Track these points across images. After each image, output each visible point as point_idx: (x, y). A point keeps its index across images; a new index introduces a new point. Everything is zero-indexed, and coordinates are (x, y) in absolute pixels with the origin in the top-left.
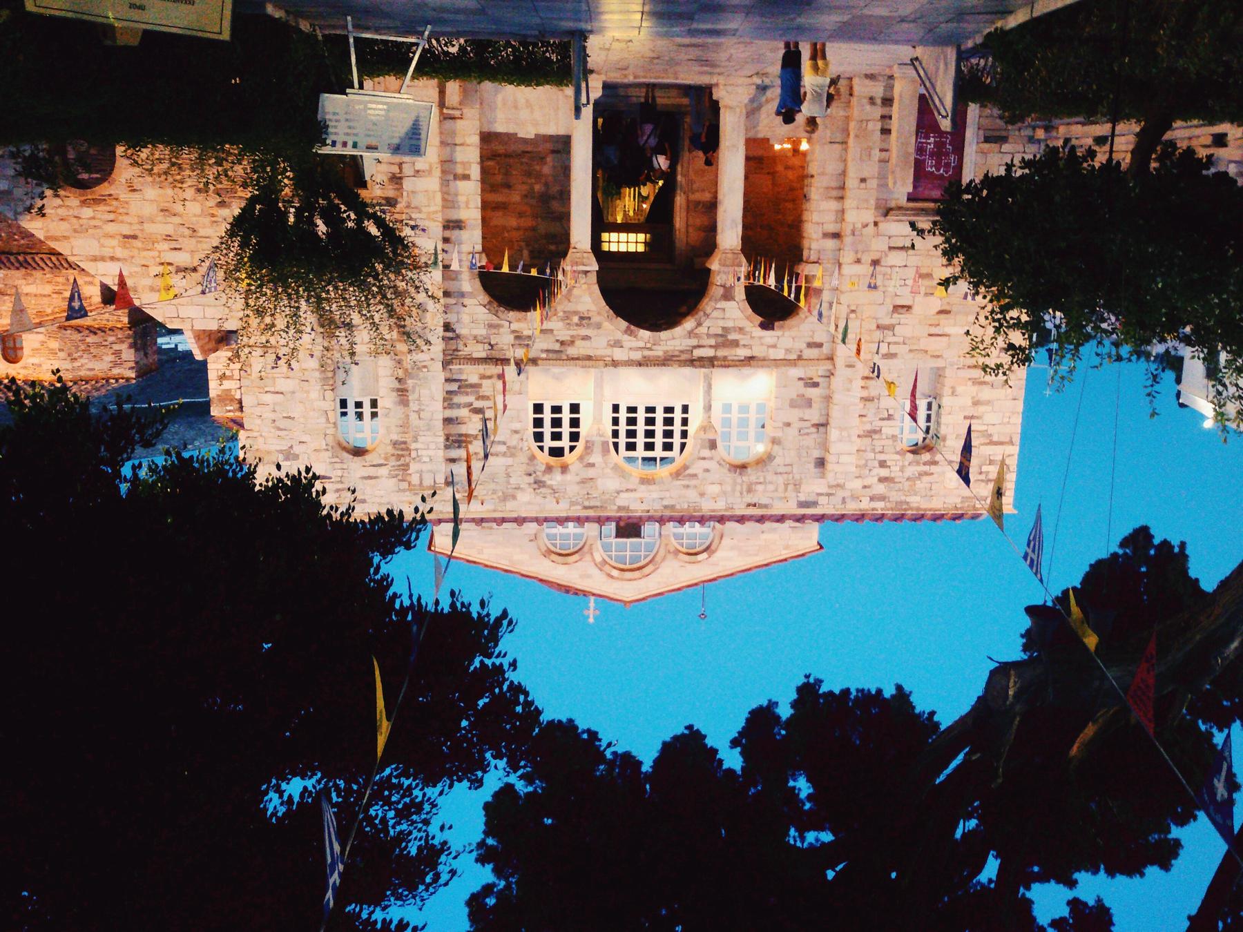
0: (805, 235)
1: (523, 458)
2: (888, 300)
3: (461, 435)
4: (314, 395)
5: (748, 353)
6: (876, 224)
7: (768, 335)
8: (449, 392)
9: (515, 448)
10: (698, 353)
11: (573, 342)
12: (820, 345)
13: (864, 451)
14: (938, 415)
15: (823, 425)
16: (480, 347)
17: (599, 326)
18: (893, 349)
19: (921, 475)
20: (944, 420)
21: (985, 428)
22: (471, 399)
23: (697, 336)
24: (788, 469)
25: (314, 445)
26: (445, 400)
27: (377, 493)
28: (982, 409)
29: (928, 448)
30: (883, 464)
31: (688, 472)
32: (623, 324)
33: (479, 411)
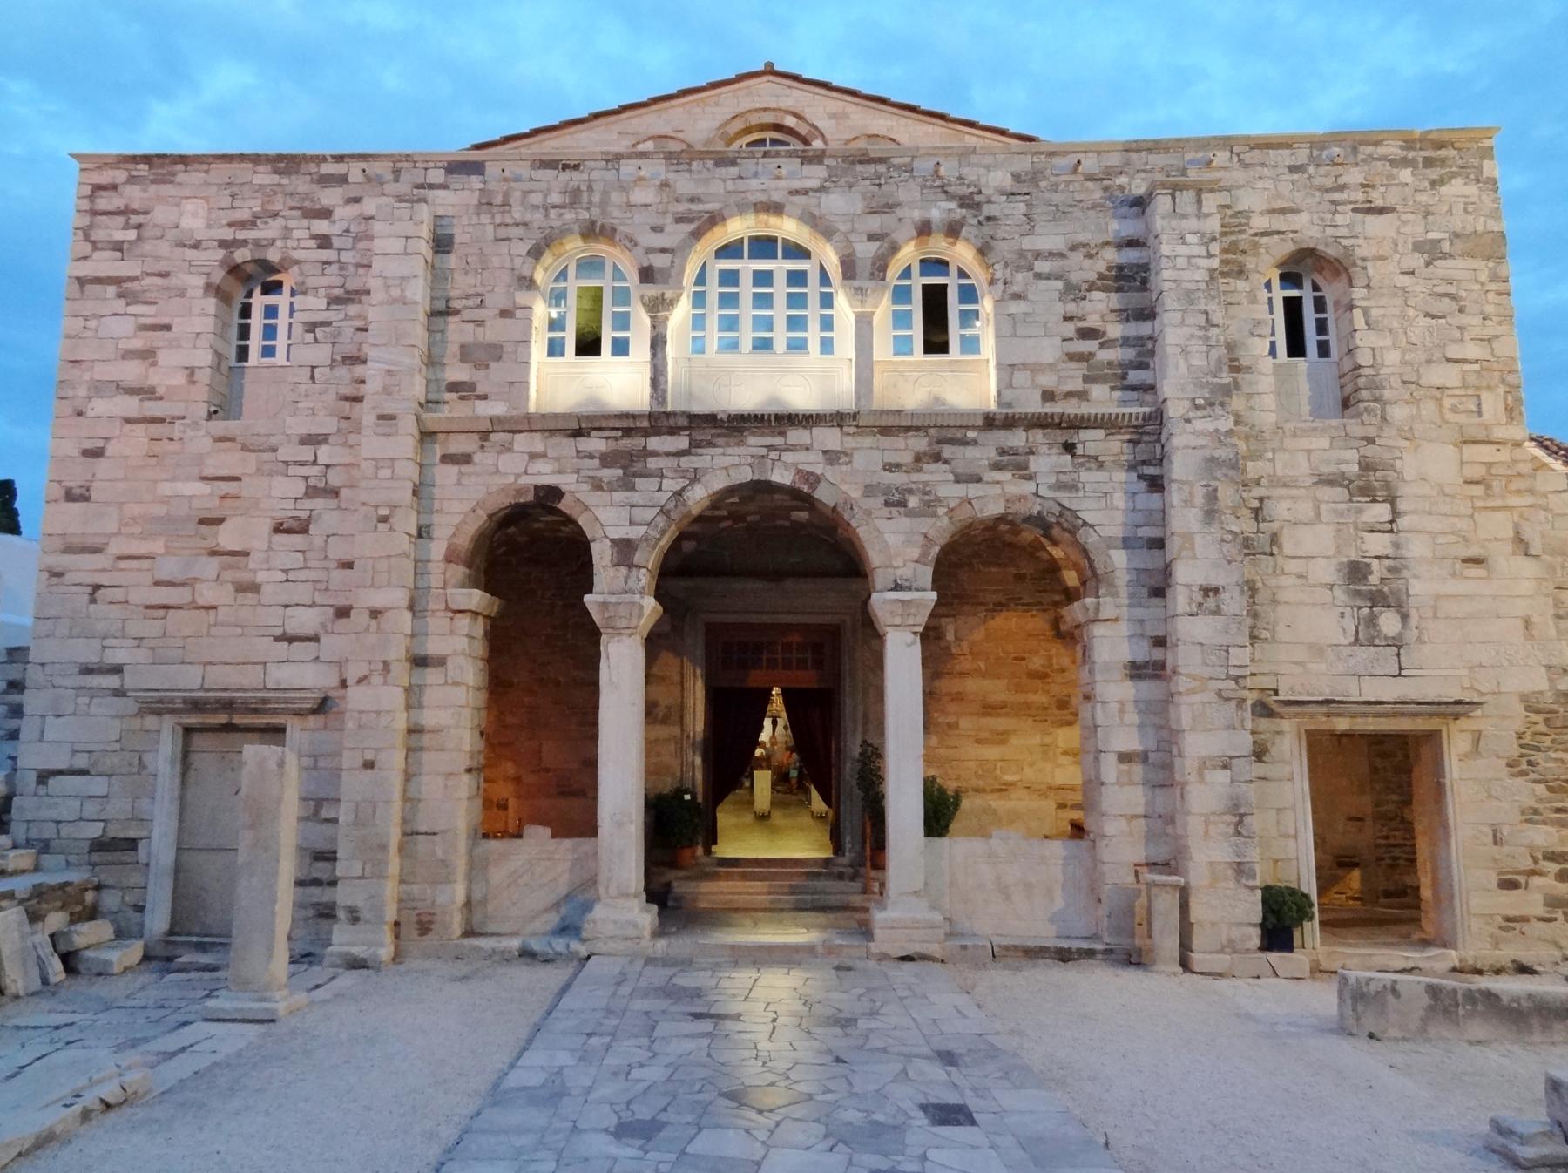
0: (481, 664)
1: (1002, 248)
2: (318, 542)
3: (1119, 290)
4: (1392, 358)
5: (586, 444)
6: (343, 684)
7: (544, 474)
8: (1142, 366)
9: (1018, 269)
10: (682, 442)
11: (918, 459)
12: (447, 459)
13: (358, 265)
14: (221, 334)
15: (441, 312)
16: (1091, 449)
17: (869, 490)
18: (306, 453)
19: (251, 223)
20: (209, 324)
21: (132, 309)
22: (1104, 355)
23: (681, 473)
24: (502, 233)
25: (1391, 267)
26: (1152, 353)
27: (1269, 184)
28: (138, 344)
29: (234, 270)
30: (324, 242)
31: (692, 227)
32: (823, 495)
33: (1087, 334)
